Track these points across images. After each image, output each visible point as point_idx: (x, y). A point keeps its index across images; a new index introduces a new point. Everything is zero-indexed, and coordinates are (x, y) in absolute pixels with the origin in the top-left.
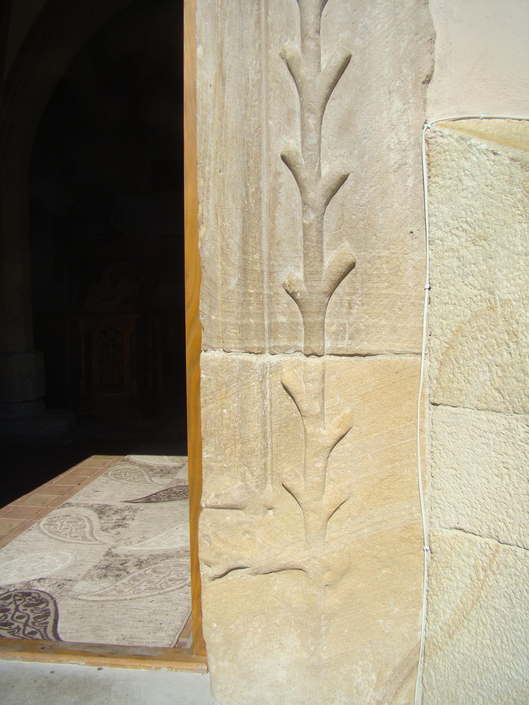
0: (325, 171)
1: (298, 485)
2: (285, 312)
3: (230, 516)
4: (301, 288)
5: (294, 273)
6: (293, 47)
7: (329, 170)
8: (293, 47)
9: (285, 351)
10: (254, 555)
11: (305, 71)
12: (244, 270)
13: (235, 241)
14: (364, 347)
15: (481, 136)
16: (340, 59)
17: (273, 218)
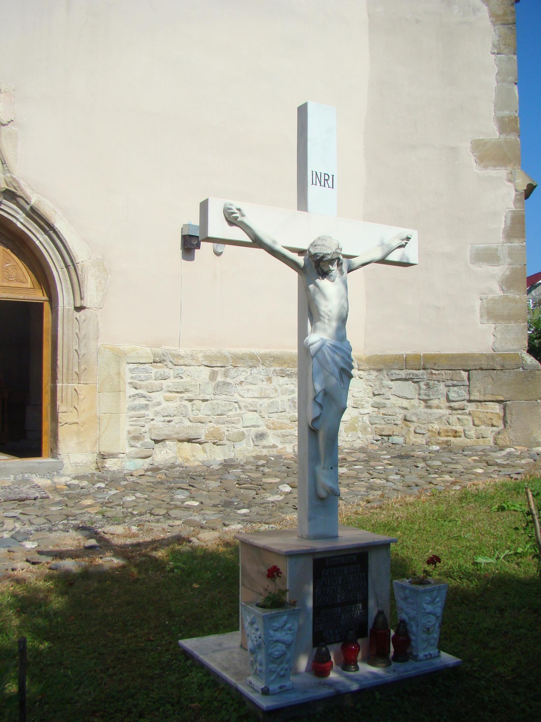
2: (75, 376)
3: (64, 414)
4: (78, 372)
5: (76, 369)
6: (77, 331)
8: (77, 331)
9: (74, 383)
11: (79, 336)
12: (68, 369)
14: (88, 383)
15: (107, 348)
17: (73, 360)
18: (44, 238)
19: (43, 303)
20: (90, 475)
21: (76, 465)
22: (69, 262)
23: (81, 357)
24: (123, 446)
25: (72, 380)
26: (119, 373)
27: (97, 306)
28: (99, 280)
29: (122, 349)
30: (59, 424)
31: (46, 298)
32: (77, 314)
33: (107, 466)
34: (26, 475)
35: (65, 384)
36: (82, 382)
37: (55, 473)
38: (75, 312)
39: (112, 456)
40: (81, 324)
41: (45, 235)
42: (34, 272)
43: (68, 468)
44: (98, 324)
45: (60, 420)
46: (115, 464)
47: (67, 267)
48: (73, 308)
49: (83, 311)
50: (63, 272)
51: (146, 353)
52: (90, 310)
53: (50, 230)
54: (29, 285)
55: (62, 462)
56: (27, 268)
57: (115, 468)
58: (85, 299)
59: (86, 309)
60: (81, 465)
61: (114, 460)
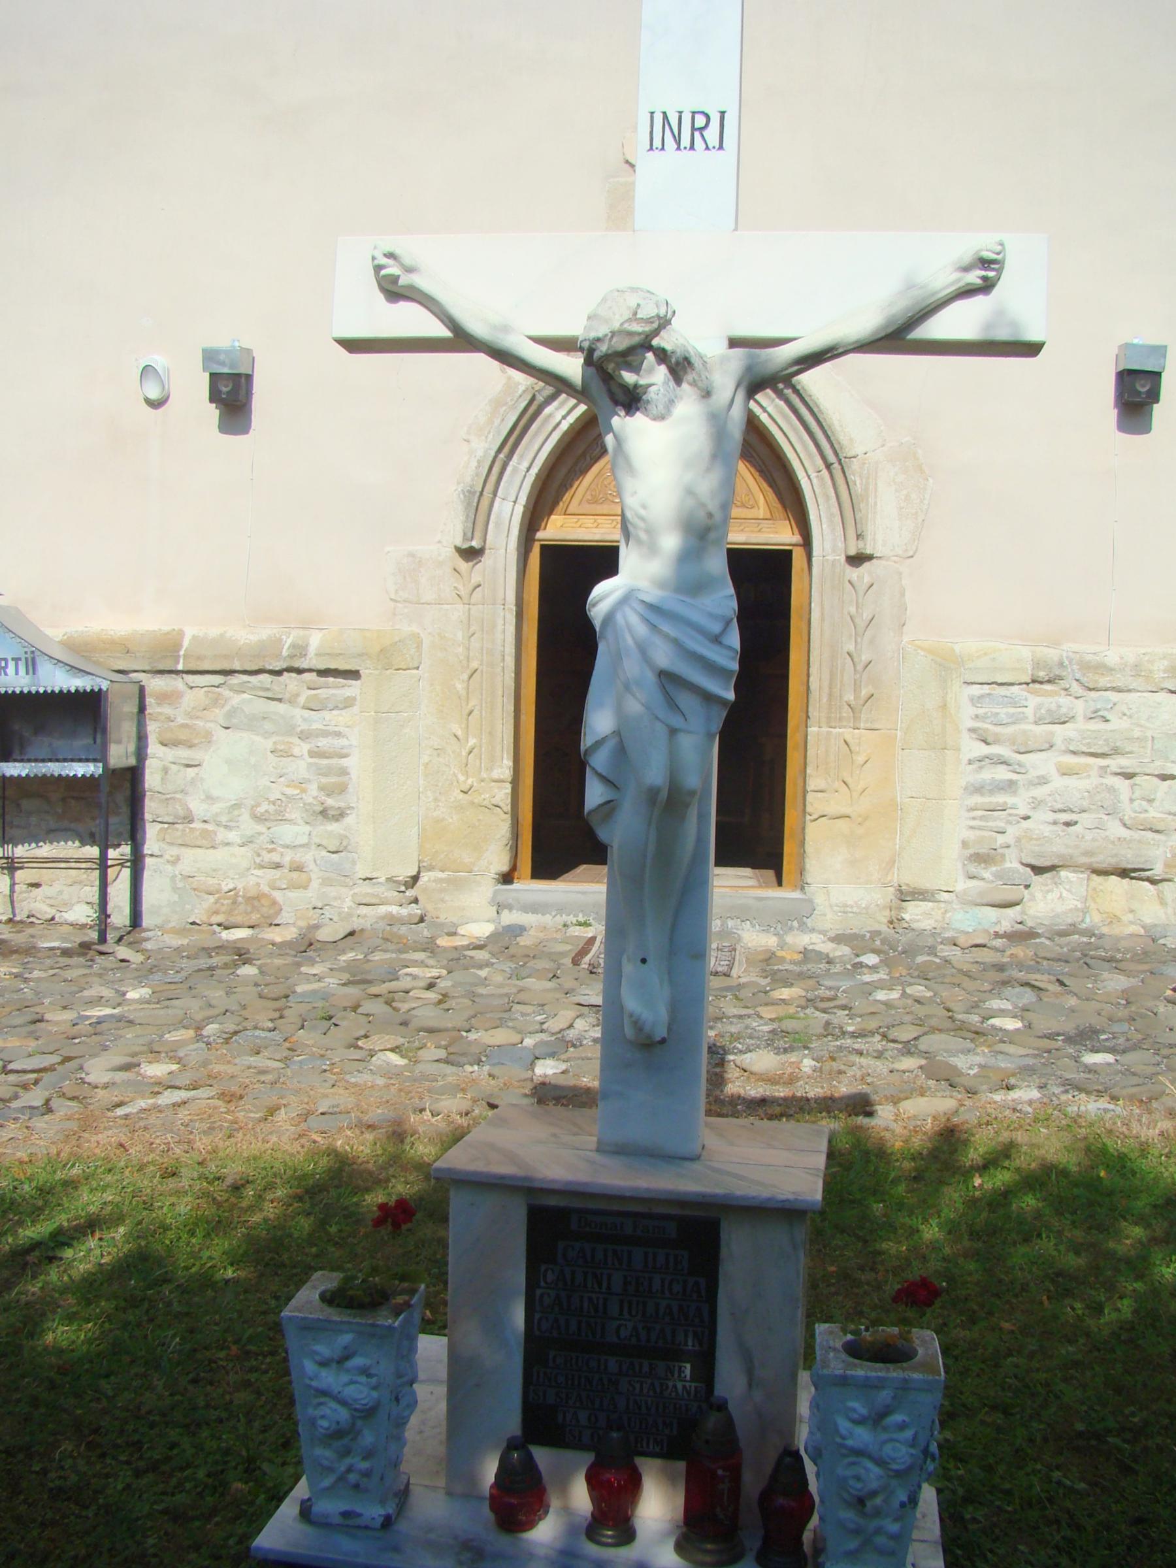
0: (863, 658)
1: (849, 780)
3: (820, 795)
4: (853, 703)
5: (850, 697)
6: (853, 610)
7: (865, 658)
8: (853, 610)
10: (832, 809)
11: (857, 620)
12: (830, 695)
13: (826, 684)
15: (922, 649)
16: (870, 617)
18: (776, 406)
19: (789, 553)
20: (868, 935)
21: (844, 909)
22: (831, 458)
23: (860, 667)
24: (949, 873)
25: (840, 719)
26: (944, 706)
27: (900, 552)
28: (905, 492)
29: (957, 651)
30: (808, 818)
31: (797, 538)
32: (854, 573)
33: (906, 916)
34: (730, 923)
35: (825, 729)
36: (862, 725)
37: (795, 924)
38: (847, 566)
39: (920, 895)
40: (861, 593)
41: (777, 400)
42: (772, 484)
43: (825, 915)
44: (903, 595)
45: (809, 809)
46: (928, 915)
47: (828, 466)
48: (843, 558)
49: (866, 565)
50: (821, 479)
51: (1019, 657)
52: (883, 562)
53: (786, 387)
54: (762, 511)
55: (811, 901)
56: (757, 475)
57: (927, 924)
58: (869, 538)
59: (874, 561)
60: (855, 910)
61: (927, 906)
